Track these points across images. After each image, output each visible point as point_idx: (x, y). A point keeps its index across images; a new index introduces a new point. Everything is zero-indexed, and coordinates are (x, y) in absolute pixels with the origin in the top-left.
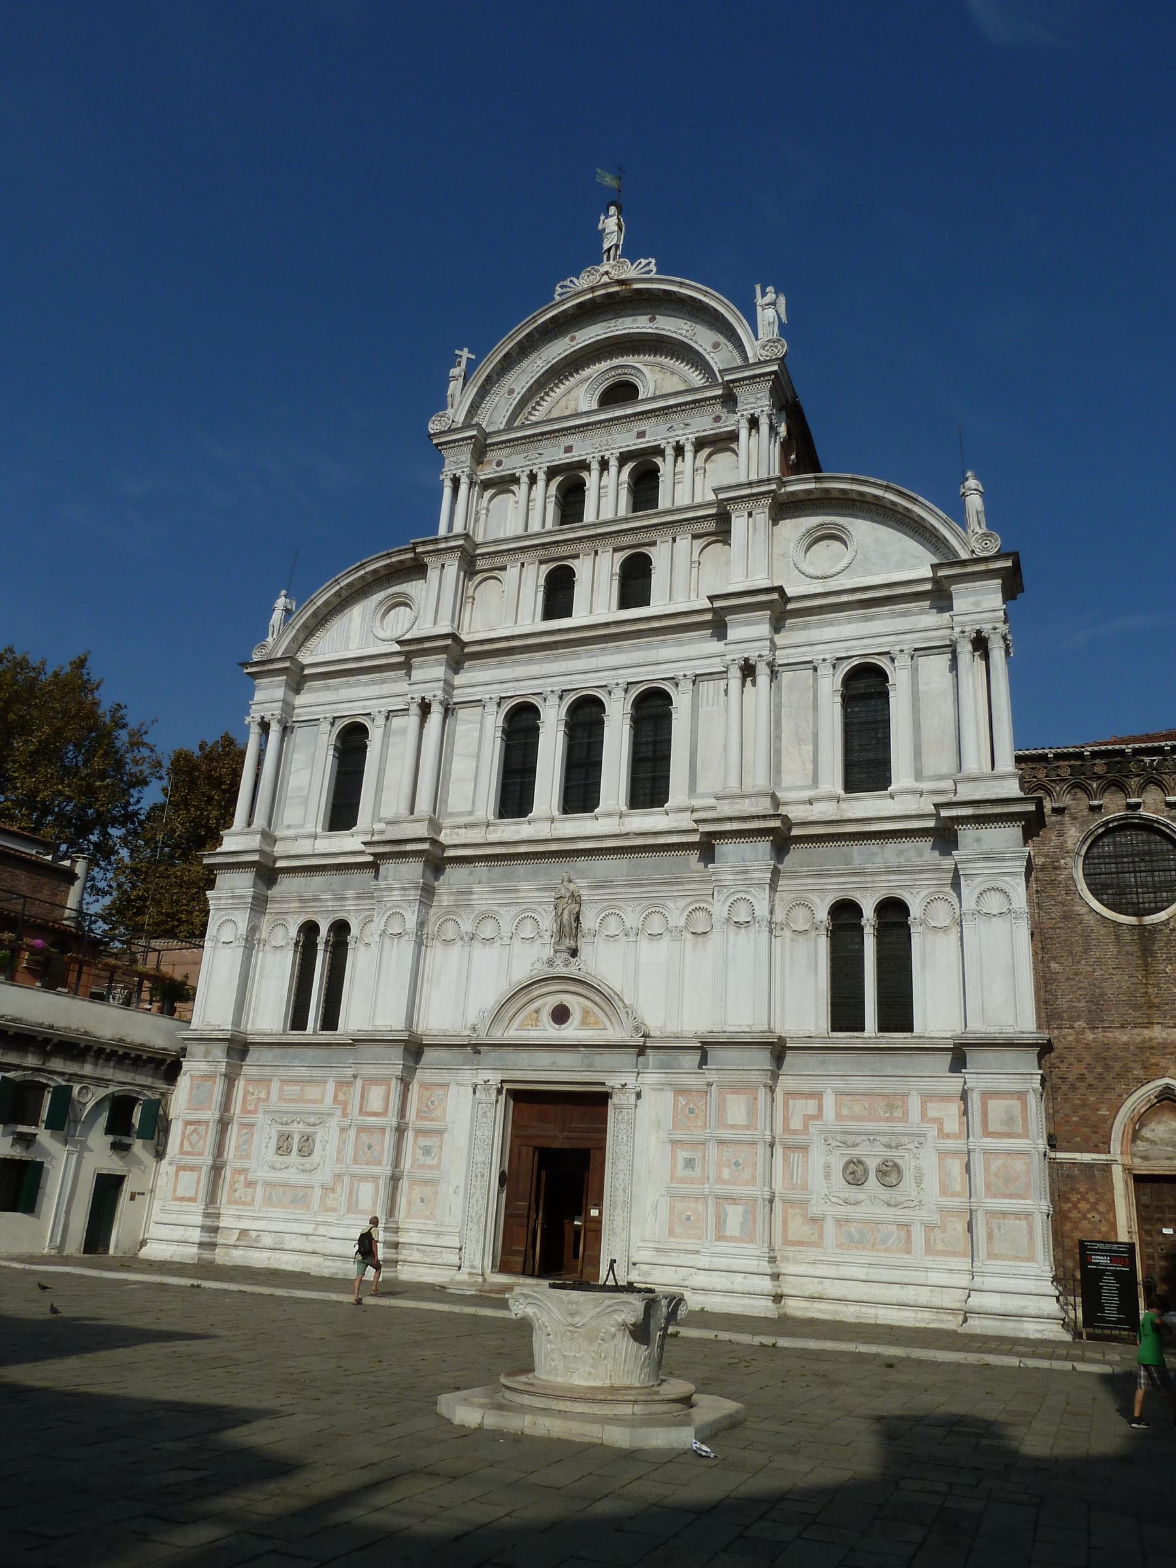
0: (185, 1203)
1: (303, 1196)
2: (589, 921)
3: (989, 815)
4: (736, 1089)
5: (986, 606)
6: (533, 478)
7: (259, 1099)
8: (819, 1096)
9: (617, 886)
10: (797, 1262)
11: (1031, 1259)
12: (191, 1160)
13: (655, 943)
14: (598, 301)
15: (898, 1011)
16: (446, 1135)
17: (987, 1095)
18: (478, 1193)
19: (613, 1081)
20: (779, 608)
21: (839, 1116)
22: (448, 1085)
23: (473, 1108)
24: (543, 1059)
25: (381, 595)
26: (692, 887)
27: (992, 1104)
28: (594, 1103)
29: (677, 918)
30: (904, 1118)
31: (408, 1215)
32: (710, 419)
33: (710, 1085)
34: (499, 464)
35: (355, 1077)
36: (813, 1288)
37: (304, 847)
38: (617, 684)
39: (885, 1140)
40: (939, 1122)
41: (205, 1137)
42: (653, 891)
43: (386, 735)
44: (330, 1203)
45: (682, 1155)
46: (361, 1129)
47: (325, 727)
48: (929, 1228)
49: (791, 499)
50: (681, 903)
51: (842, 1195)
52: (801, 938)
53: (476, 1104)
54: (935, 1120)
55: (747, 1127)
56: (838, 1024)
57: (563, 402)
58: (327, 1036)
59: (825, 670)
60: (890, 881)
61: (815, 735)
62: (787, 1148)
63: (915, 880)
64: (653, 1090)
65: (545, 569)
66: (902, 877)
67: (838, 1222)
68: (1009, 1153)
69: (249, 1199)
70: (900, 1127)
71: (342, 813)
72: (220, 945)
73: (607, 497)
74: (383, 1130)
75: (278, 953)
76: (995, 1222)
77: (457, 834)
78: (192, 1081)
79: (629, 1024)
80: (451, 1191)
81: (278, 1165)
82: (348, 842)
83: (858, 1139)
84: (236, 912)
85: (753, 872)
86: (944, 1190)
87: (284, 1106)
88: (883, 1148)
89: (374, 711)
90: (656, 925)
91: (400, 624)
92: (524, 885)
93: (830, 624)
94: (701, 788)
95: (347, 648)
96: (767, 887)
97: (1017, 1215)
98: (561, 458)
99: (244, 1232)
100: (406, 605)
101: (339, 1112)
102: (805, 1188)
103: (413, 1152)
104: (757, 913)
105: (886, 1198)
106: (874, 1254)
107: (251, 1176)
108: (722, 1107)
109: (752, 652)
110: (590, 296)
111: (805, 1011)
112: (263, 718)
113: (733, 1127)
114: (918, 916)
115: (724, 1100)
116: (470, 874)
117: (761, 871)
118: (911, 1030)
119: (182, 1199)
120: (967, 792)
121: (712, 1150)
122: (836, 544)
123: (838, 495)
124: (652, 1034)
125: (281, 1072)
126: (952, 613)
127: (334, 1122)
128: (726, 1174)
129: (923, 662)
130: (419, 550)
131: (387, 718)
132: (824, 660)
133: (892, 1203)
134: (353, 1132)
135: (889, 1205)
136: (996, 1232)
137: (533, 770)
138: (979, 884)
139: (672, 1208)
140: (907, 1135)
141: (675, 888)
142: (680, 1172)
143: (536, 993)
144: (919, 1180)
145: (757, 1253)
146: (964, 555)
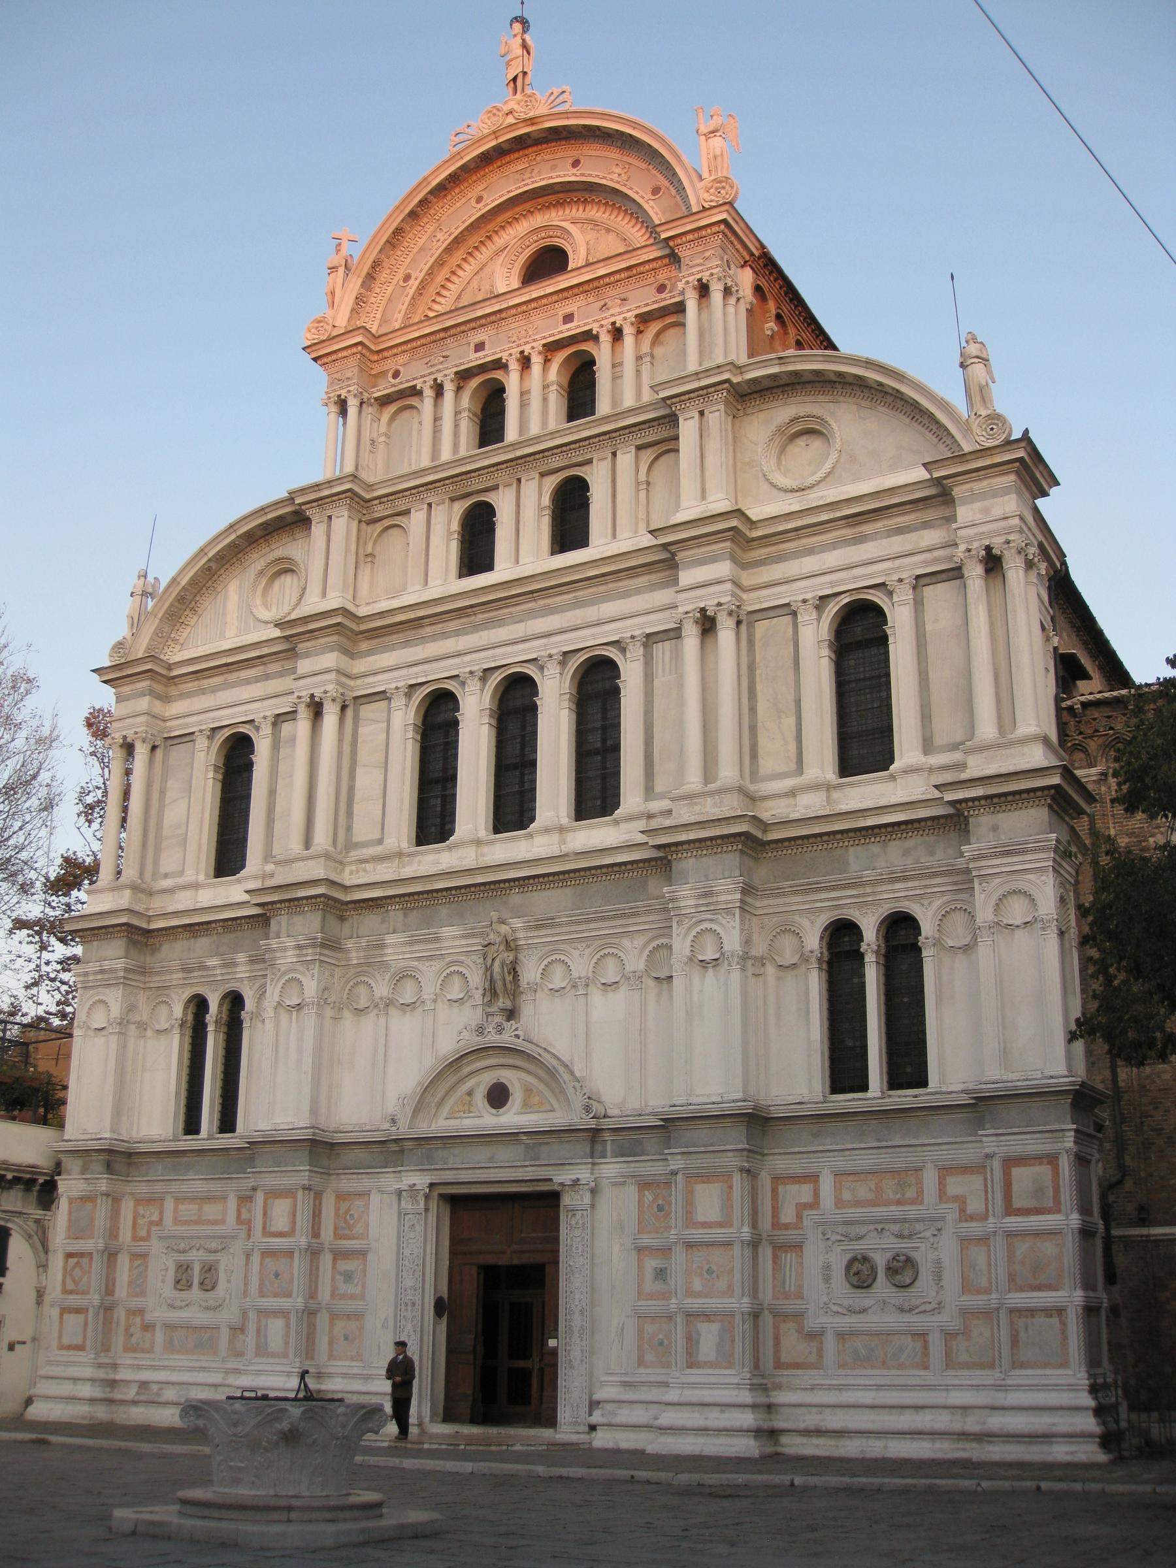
0: (74, 1352)
2: (530, 972)
3: (1004, 796)
4: (705, 1177)
5: (997, 512)
6: (439, 390)
7: (151, 1223)
8: (813, 1178)
9: (559, 925)
10: (790, 1388)
11: (1064, 1365)
12: (74, 1301)
13: (610, 995)
14: (506, 147)
15: (908, 1065)
16: (370, 1257)
17: (1010, 1162)
18: (409, 1326)
19: (563, 1177)
20: (738, 536)
21: (839, 1203)
22: (365, 1195)
23: (399, 1220)
24: (479, 1154)
25: (260, 564)
26: (651, 918)
27: (1016, 1172)
28: (543, 1204)
29: (636, 961)
30: (918, 1200)
31: (331, 1357)
32: (652, 290)
33: (674, 1173)
34: (396, 375)
35: (254, 1189)
36: (810, 1420)
37: (184, 901)
38: (550, 656)
39: (895, 1228)
40: (961, 1200)
41: (90, 1272)
42: (604, 928)
43: (276, 746)
45: (651, 1263)
46: (267, 1253)
47: (201, 743)
48: (949, 1336)
49: (754, 388)
50: (639, 941)
51: (846, 1302)
52: (789, 975)
53: (402, 1215)
54: (956, 1199)
55: (720, 1225)
56: (837, 1086)
57: (474, 284)
58: (225, 1141)
59: (806, 616)
60: (894, 891)
61: (798, 703)
62: (779, 1248)
63: (926, 886)
64: (614, 1184)
65: (460, 508)
66: (910, 884)
67: (841, 1336)
68: (1037, 1234)
69: (147, 1345)
70: (912, 1211)
71: (228, 856)
72: (91, 1033)
73: (535, 408)
74: (290, 1254)
75: (163, 1038)
76: (1021, 1323)
77: (365, 870)
78: (70, 1203)
79: (578, 1102)
80: (379, 1325)
81: (178, 1303)
82: (233, 893)
83: (863, 1230)
84: (107, 991)
85: (718, 894)
86: (967, 1287)
87: (181, 1230)
88: (893, 1240)
89: (257, 717)
90: (611, 972)
91: (287, 598)
92: (447, 931)
93: (810, 551)
94: (659, 787)
95: (223, 636)
96: (737, 911)
97: (1048, 1311)
98: (474, 359)
99: (144, 1385)
100: (293, 571)
101: (243, 1235)
102: (800, 1295)
103: (333, 1279)
104: (726, 948)
105: (897, 1302)
106: (885, 1372)
107: (148, 1317)
108: (689, 1202)
109: (709, 599)
110: (493, 143)
111: (796, 1072)
112: (125, 737)
113: (704, 1225)
114: (930, 934)
115: (691, 1192)
116: (383, 921)
117: (728, 892)
118: (924, 1083)
119: (69, 1348)
120: (978, 766)
121: (679, 1255)
122: (816, 444)
123: (811, 378)
124: (610, 1112)
125: (174, 1187)
126: (954, 526)
127: (239, 1246)
128: (697, 1286)
129: (928, 591)
130: (298, 501)
131: (274, 724)
132: (804, 601)
133: (906, 1307)
134: (256, 1258)
135: (902, 1310)
136: (1022, 1335)
137: (454, 778)
138: (997, 887)
139: (640, 1331)
140: (922, 1220)
141: (631, 921)
142: (650, 1286)
143: (466, 1070)
144: (938, 1277)
145: (735, 1381)
146: (967, 447)
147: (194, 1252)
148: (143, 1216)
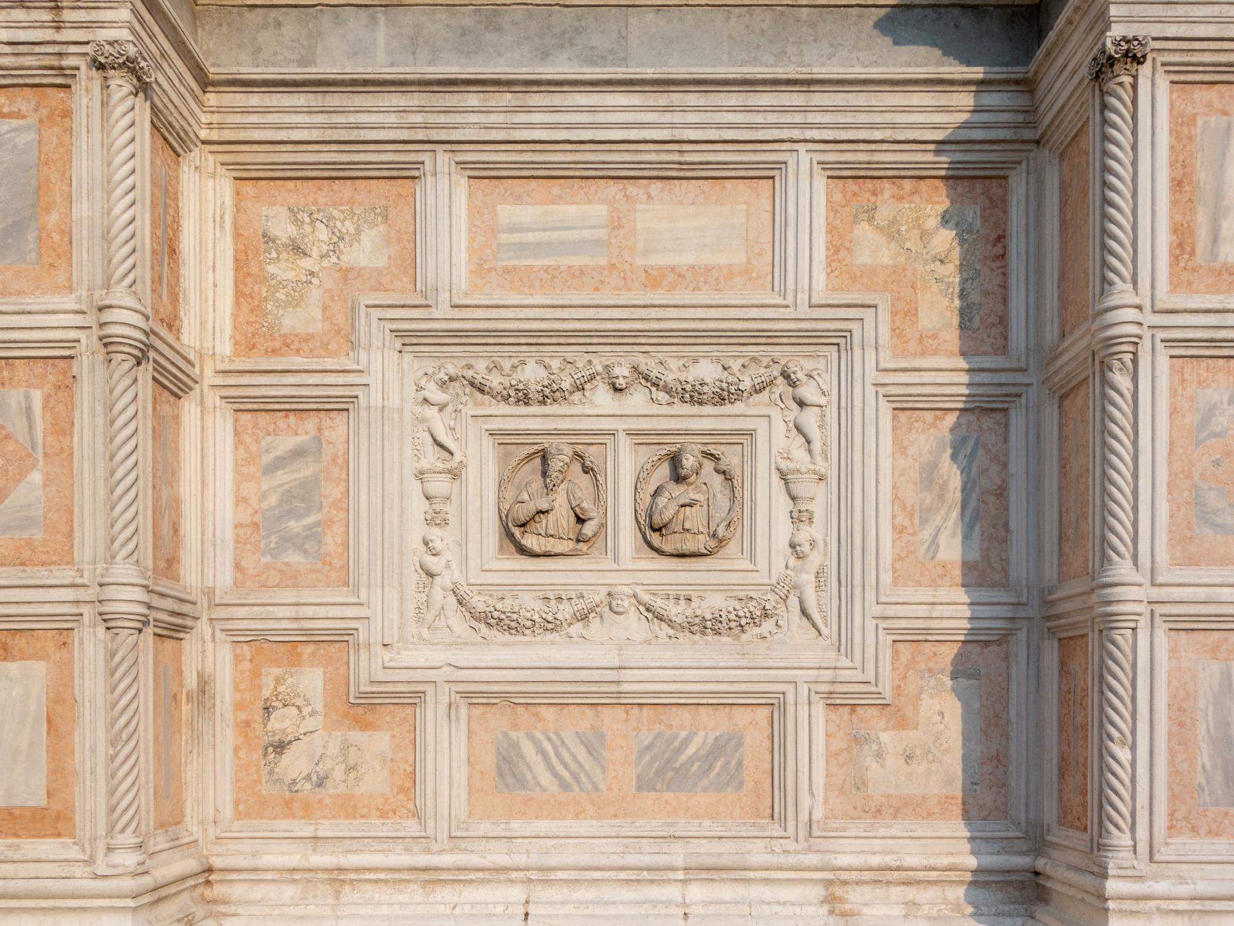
1: (718, 749)
7: (346, 273)
44: (885, 773)
69: (375, 782)
81: (530, 605)
87: (525, 305)
147: (602, 398)
148: (298, 249)
